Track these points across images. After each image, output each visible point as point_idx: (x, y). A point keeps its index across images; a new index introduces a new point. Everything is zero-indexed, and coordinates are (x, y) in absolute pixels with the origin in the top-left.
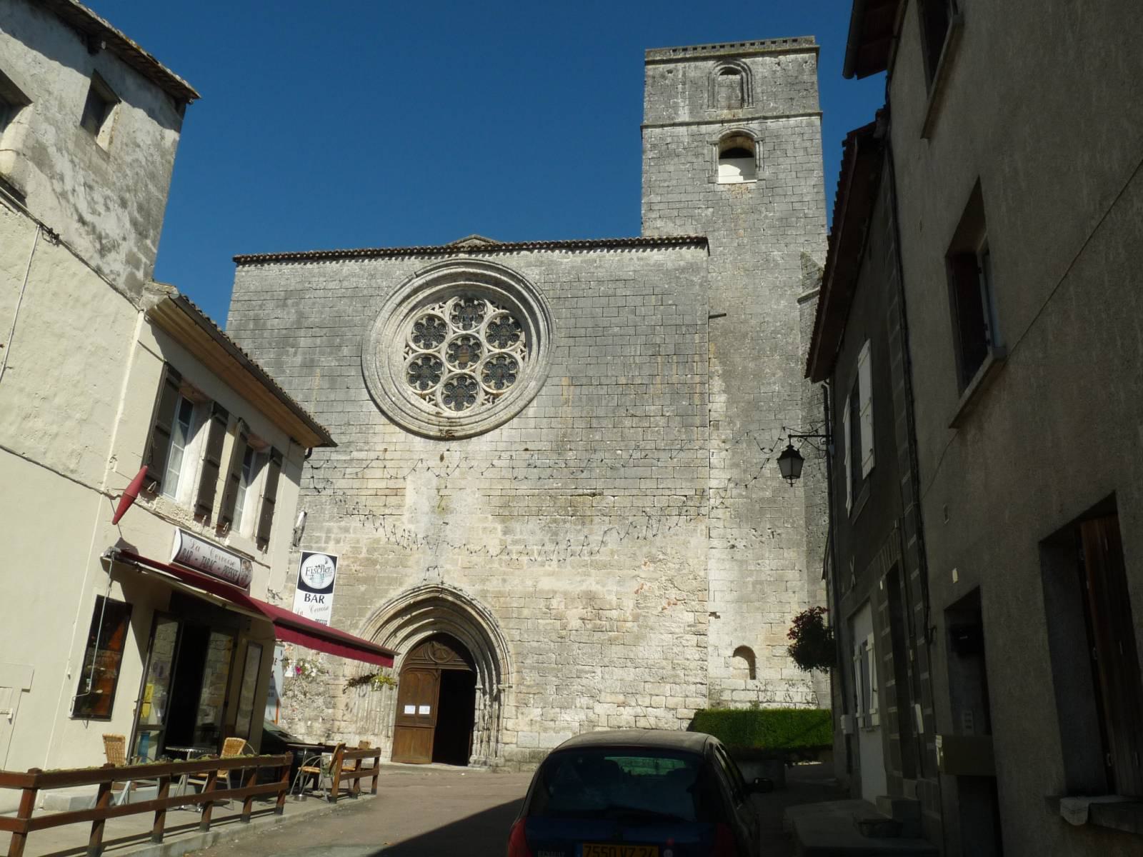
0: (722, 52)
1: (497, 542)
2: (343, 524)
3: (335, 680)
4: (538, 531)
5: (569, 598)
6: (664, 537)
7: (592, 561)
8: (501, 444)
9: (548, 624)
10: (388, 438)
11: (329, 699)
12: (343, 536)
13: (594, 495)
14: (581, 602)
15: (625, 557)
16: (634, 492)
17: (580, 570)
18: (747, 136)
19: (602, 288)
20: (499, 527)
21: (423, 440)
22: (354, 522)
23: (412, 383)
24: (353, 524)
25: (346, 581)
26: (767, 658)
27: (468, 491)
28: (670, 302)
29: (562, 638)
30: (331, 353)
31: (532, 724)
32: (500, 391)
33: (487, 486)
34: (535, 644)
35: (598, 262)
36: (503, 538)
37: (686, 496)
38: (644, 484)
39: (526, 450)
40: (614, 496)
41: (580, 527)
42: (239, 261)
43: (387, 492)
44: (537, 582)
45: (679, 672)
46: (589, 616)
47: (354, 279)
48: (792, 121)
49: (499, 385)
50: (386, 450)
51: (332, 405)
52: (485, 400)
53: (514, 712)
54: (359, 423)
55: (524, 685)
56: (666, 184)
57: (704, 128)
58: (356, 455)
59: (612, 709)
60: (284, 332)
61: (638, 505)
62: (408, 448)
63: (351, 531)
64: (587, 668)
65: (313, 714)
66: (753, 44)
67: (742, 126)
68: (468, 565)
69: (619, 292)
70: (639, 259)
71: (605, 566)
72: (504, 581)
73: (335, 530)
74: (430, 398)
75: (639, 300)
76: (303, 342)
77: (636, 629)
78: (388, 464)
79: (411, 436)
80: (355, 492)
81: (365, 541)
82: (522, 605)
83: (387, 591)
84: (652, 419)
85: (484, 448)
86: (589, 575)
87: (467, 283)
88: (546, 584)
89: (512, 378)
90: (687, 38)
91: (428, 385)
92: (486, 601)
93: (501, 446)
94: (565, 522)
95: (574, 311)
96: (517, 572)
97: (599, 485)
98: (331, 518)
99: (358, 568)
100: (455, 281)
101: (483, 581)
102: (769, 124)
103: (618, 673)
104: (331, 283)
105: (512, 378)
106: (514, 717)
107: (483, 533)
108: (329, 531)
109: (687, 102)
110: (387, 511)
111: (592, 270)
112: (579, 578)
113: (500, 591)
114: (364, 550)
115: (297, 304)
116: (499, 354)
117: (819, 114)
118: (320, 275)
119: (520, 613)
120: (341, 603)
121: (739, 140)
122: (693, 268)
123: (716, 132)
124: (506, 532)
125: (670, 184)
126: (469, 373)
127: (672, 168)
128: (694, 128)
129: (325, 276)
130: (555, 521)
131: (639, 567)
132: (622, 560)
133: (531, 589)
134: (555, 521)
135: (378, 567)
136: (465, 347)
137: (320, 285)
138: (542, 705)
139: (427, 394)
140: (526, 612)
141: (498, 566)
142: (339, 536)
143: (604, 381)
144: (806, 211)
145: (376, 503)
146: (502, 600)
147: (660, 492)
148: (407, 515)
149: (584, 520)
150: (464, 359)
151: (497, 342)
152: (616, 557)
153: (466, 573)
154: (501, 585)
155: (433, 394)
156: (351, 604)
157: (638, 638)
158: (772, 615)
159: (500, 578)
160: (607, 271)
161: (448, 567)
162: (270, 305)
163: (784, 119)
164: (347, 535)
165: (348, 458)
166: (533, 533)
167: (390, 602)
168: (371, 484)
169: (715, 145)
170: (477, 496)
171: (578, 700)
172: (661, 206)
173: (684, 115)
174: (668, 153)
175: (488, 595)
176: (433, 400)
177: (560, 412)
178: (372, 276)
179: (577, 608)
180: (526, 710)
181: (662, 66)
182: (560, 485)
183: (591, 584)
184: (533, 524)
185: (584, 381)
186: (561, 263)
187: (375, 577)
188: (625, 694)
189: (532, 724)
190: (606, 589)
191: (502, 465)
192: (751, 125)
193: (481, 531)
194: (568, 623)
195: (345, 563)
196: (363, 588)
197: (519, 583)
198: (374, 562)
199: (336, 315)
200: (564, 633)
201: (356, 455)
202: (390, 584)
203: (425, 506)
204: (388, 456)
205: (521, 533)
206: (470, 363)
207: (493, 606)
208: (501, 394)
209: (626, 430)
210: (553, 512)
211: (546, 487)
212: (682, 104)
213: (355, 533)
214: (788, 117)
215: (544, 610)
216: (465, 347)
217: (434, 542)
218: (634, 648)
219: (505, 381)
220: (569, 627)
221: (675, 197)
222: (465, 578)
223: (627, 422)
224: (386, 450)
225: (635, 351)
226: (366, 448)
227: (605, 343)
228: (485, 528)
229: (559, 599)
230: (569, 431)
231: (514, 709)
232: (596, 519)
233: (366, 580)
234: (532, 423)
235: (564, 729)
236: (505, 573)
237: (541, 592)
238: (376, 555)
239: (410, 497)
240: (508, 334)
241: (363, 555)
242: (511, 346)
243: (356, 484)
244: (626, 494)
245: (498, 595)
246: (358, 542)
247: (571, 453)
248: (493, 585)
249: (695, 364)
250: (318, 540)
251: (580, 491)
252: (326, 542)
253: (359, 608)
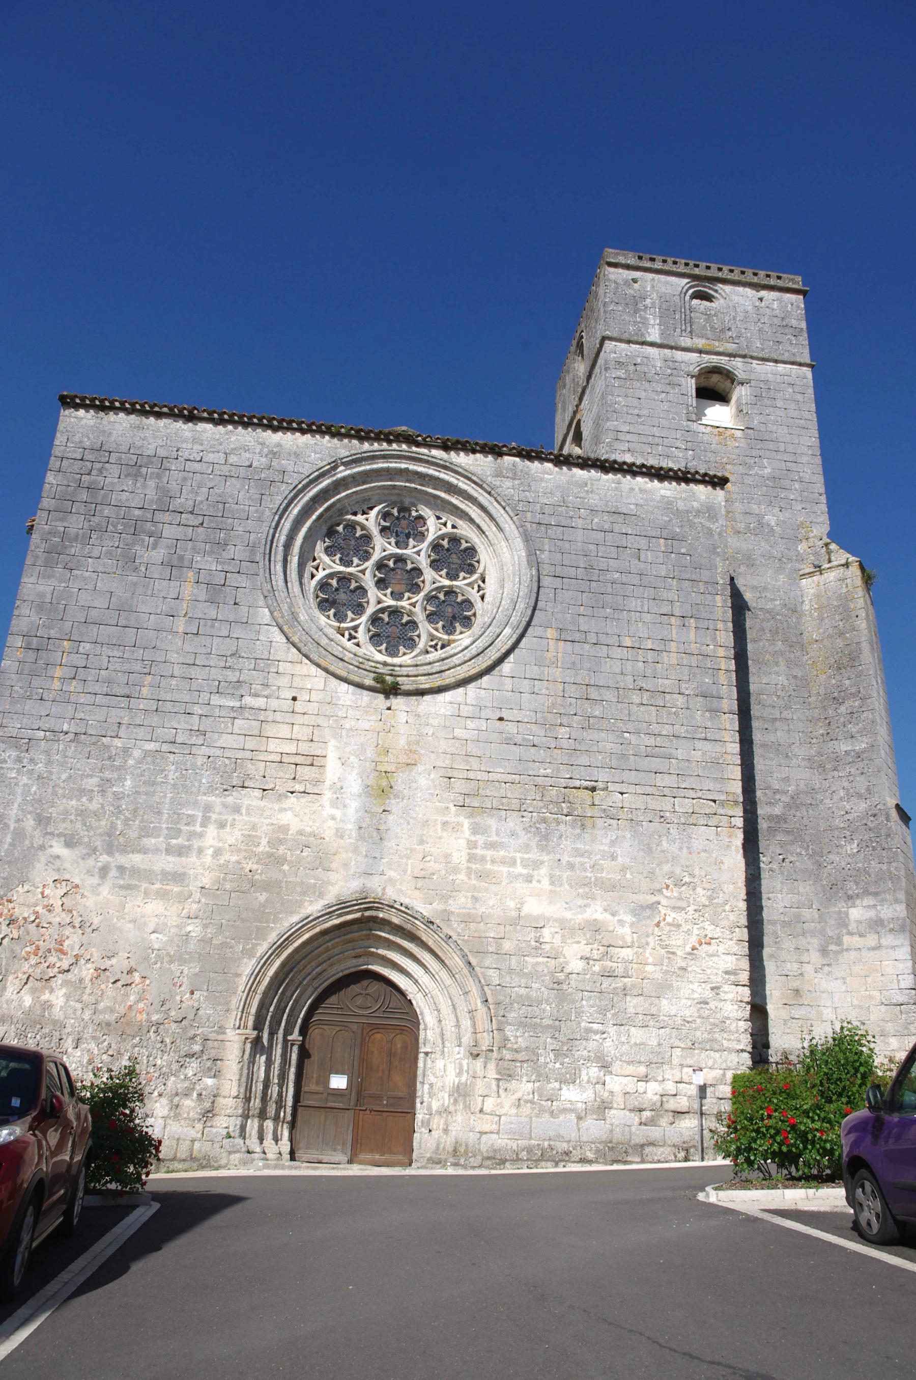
0: (697, 271)
1: (463, 843)
2: (230, 800)
3: (218, 1033)
4: (522, 833)
5: (568, 929)
6: (690, 853)
7: (596, 879)
8: (466, 708)
9: (537, 963)
10: (297, 682)
11: (209, 1064)
12: (230, 818)
13: (593, 789)
14: (584, 935)
15: (641, 877)
16: (649, 790)
17: (581, 891)
18: (729, 376)
19: (596, 520)
20: (466, 823)
21: (351, 688)
22: (250, 799)
23: (324, 610)
24: (246, 802)
25: (235, 885)
26: (785, 1020)
27: (420, 768)
28: (683, 551)
29: (559, 983)
30: (212, 552)
31: (519, 1105)
32: (452, 637)
33: (447, 763)
34: (523, 991)
35: (589, 486)
36: (473, 838)
37: (715, 801)
38: (660, 780)
39: (501, 719)
40: (622, 794)
41: (578, 831)
42: (68, 402)
43: (299, 760)
44: (522, 904)
45: (717, 1035)
46: (596, 955)
47: (247, 455)
48: (781, 367)
49: (449, 629)
50: (294, 699)
51: (213, 626)
52: (431, 646)
53: (494, 1087)
54: (254, 655)
55: (509, 1049)
56: (636, 411)
57: (679, 355)
58: (248, 700)
59: (630, 1084)
60: (137, 512)
61: (654, 807)
62: (328, 699)
63: (244, 811)
64: (595, 1026)
65: (181, 1086)
66: (731, 271)
67: (723, 361)
68: (422, 874)
69: (617, 528)
70: (641, 490)
71: (613, 888)
72: (475, 899)
73: (218, 809)
74: (350, 634)
75: (643, 543)
76: (169, 532)
77: (658, 975)
78: (299, 719)
79: (333, 682)
80: (248, 754)
81: (265, 827)
82: (502, 935)
83: (300, 904)
84: (667, 696)
85: (443, 711)
86: (594, 898)
87: (407, 484)
88: (533, 907)
89: (467, 622)
90: (656, 244)
91: (346, 615)
92: (450, 926)
93: (466, 711)
94: (558, 823)
95: (560, 543)
96: (494, 888)
97: (603, 776)
98: (211, 790)
99: (255, 867)
100: (391, 480)
101: (445, 898)
102: (754, 365)
103: (637, 1034)
104: (210, 455)
105: (467, 622)
106: (494, 1094)
107: (443, 830)
108: (208, 808)
109: (658, 321)
110: (298, 787)
111: (581, 495)
112: (580, 902)
113: (469, 914)
114: (264, 842)
115: (159, 476)
116: (449, 587)
117: (812, 366)
118: (195, 440)
119: (499, 946)
120: (227, 917)
121: (715, 378)
122: (710, 511)
123: (692, 361)
124: (475, 830)
125: (641, 413)
126: (408, 607)
127: (643, 395)
128: (667, 352)
129: (202, 444)
130: (544, 821)
131: (660, 891)
132: (636, 880)
133: (514, 914)
134: (544, 821)
135: (286, 867)
136: (399, 572)
137: (195, 455)
138: (534, 1077)
139: (348, 629)
140: (507, 946)
141: (466, 879)
142: (224, 817)
143: (603, 639)
144: (801, 474)
145: (281, 774)
146: (472, 925)
147: (682, 793)
148: (328, 795)
149: (582, 822)
150: (398, 588)
151: (445, 570)
152: (628, 876)
153: (419, 885)
154: (470, 905)
155: (355, 628)
156: (243, 921)
157: (663, 988)
158: (789, 965)
159: (469, 894)
160: (601, 499)
161: (392, 874)
162: (114, 470)
163: (771, 364)
164: (236, 817)
165: (238, 704)
166: (513, 834)
167: (307, 922)
168: (273, 746)
169: (692, 377)
170: (432, 776)
171: (584, 1072)
172: (629, 437)
173: (654, 335)
174: (636, 373)
175: (452, 918)
176: (355, 638)
177: (546, 672)
178: (273, 454)
179: (579, 942)
180: (514, 1084)
181: (626, 272)
182: (549, 771)
183: (596, 912)
184: (513, 822)
185: (577, 636)
186: (542, 480)
187: (281, 881)
188: (649, 1064)
189: (519, 1105)
190: (616, 918)
191: (468, 736)
192: (734, 363)
193: (439, 826)
194: (567, 963)
195: (234, 858)
196: (262, 897)
197: (493, 903)
198: (280, 861)
199: (219, 499)
200: (561, 976)
201: (248, 700)
202: (304, 894)
203: (354, 784)
204: (299, 706)
205: (498, 834)
206: (407, 595)
207: (459, 935)
208: (454, 641)
209: (634, 708)
210: (541, 808)
211: (531, 773)
212: (652, 322)
213: (248, 814)
214: (776, 361)
215: (533, 943)
216: (399, 572)
217: (373, 832)
218: (657, 1001)
219: (457, 625)
220: (568, 969)
221: (647, 430)
222: (417, 892)
223: (636, 698)
224: (294, 699)
225: (642, 605)
226: (266, 693)
227: (602, 590)
228: (445, 823)
229: (553, 930)
230: (559, 699)
231: (494, 1083)
232: (600, 822)
233: (267, 886)
234: (508, 684)
235: (564, 1110)
236: (475, 888)
237: (528, 917)
238: (282, 850)
239: (332, 770)
240: (459, 562)
241: (264, 847)
242: (464, 578)
243: (251, 743)
244: (639, 791)
245: (467, 919)
246: (254, 827)
247: (563, 730)
248: (460, 903)
249: (718, 632)
250: (191, 820)
251: (577, 783)
252: (203, 825)
253: (258, 928)
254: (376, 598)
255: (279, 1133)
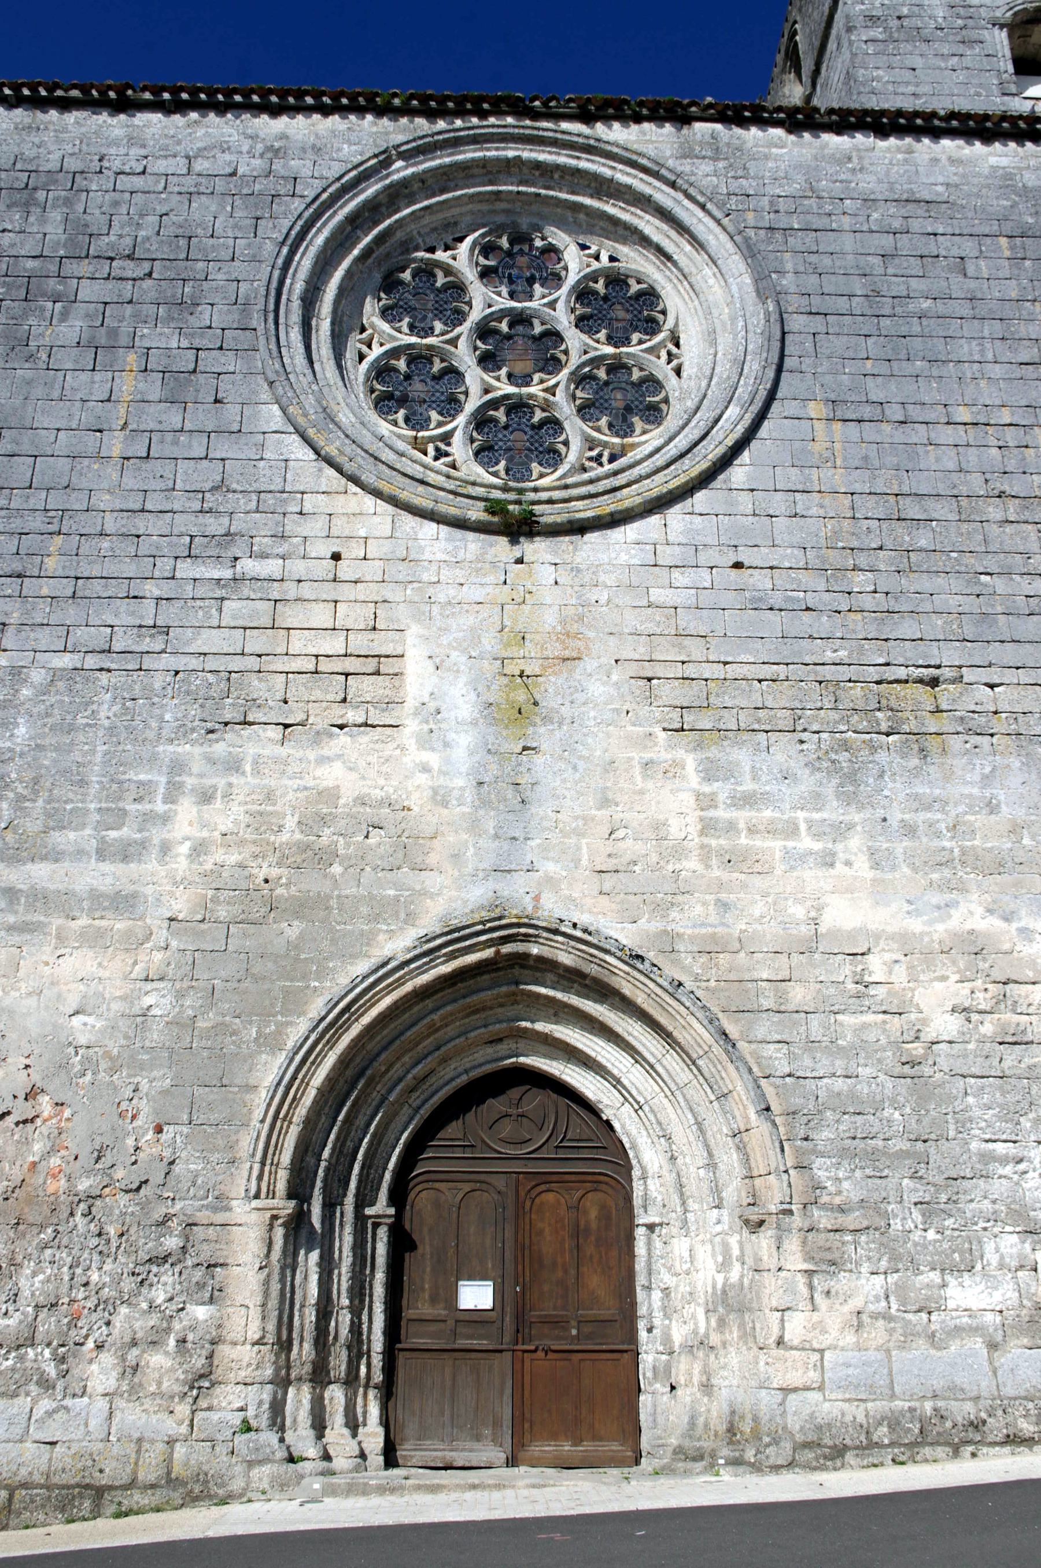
1: (688, 800)
2: (220, 748)
3: (215, 1209)
7: (964, 852)
8: (668, 550)
9: (865, 1026)
10: (340, 526)
11: (198, 1274)
12: (221, 783)
13: (934, 682)
14: (954, 962)
17: (935, 876)
19: (875, 215)
20: (690, 761)
21: (444, 529)
22: (260, 744)
24: (252, 750)
25: (237, 909)
27: (590, 664)
29: (913, 1063)
31: (860, 1326)
32: (628, 440)
33: (642, 652)
35: (855, 160)
36: (706, 789)
39: (738, 565)
40: (992, 686)
41: (915, 762)
43: (351, 665)
44: (819, 909)
47: (227, 157)
49: (622, 427)
50: (336, 557)
51: (176, 442)
52: (590, 459)
53: (804, 1291)
54: (255, 486)
55: (824, 1207)
56: (911, 89)
58: (248, 566)
60: (30, 264)
63: (248, 768)
64: (1000, 1148)
65: (142, 1325)
69: (915, 225)
70: (952, 161)
71: (999, 867)
72: (724, 906)
74: (437, 449)
75: (968, 247)
78: (346, 592)
79: (409, 521)
80: (252, 663)
81: (291, 796)
82: (785, 974)
83: (369, 939)
85: (624, 558)
88: (843, 915)
89: (654, 414)
91: (429, 419)
92: (676, 962)
93: (667, 555)
94: (874, 749)
95: (813, 258)
96: (757, 881)
97: (950, 655)
98: (182, 732)
100: (491, 183)
101: (661, 909)
105: (654, 414)
107: (645, 777)
108: (178, 767)
110: (353, 716)
111: (843, 177)
112: (936, 898)
115: (68, 202)
116: (614, 356)
118: (132, 141)
119: (782, 997)
120: (223, 974)
124: (710, 772)
125: (920, 90)
127: (918, 62)
129: (144, 146)
130: (846, 746)
133: (805, 930)
134: (846, 746)
135: (337, 869)
137: (133, 164)
138: (884, 1264)
139: (432, 440)
140: (798, 995)
142: (208, 782)
143: (914, 412)
145: (317, 694)
148: (412, 726)
150: (520, 368)
151: (604, 331)
152: (1026, 841)
153: (607, 887)
154: (713, 919)
156: (256, 979)
160: (880, 181)
161: (550, 867)
164: (233, 780)
165: (228, 574)
167: (386, 973)
168: (298, 643)
169: (1002, 26)
170: (615, 677)
171: (989, 1247)
175: (680, 947)
176: (447, 454)
178: (275, 152)
179: (944, 978)
180: (842, 1282)
183: (971, 915)
184: (783, 752)
185: (867, 412)
186: (767, 157)
187: (329, 897)
189: (860, 1326)
190: (1015, 925)
191: (678, 601)
193: (637, 770)
194: (925, 1022)
195: (234, 858)
196: (293, 930)
198: (324, 858)
200: (917, 1049)
202: (376, 918)
203: (462, 702)
204: (345, 569)
205: (755, 778)
207: (697, 979)
210: (836, 722)
215: (850, 986)
217: (506, 793)
219: (636, 419)
222: (603, 900)
223: (994, 511)
224: (336, 557)
227: (904, 330)
228: (647, 764)
229: (888, 957)
231: (801, 1280)
233: (301, 908)
235: (958, 1331)
237: (835, 934)
239: (418, 679)
240: (629, 317)
241: (290, 833)
242: (641, 342)
243: (256, 642)
246: (269, 797)
247: (861, 577)
248: (692, 918)
250: (144, 792)
251: (902, 673)
252: (170, 798)
253: (287, 992)
254: (477, 384)
255: (359, 1410)
